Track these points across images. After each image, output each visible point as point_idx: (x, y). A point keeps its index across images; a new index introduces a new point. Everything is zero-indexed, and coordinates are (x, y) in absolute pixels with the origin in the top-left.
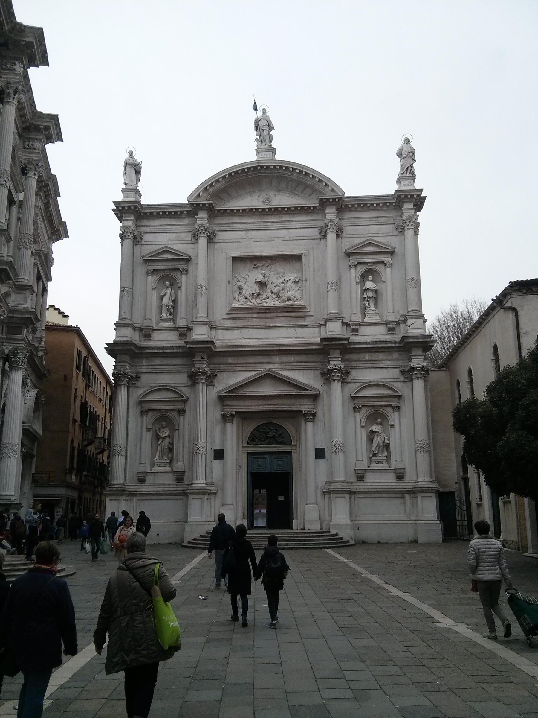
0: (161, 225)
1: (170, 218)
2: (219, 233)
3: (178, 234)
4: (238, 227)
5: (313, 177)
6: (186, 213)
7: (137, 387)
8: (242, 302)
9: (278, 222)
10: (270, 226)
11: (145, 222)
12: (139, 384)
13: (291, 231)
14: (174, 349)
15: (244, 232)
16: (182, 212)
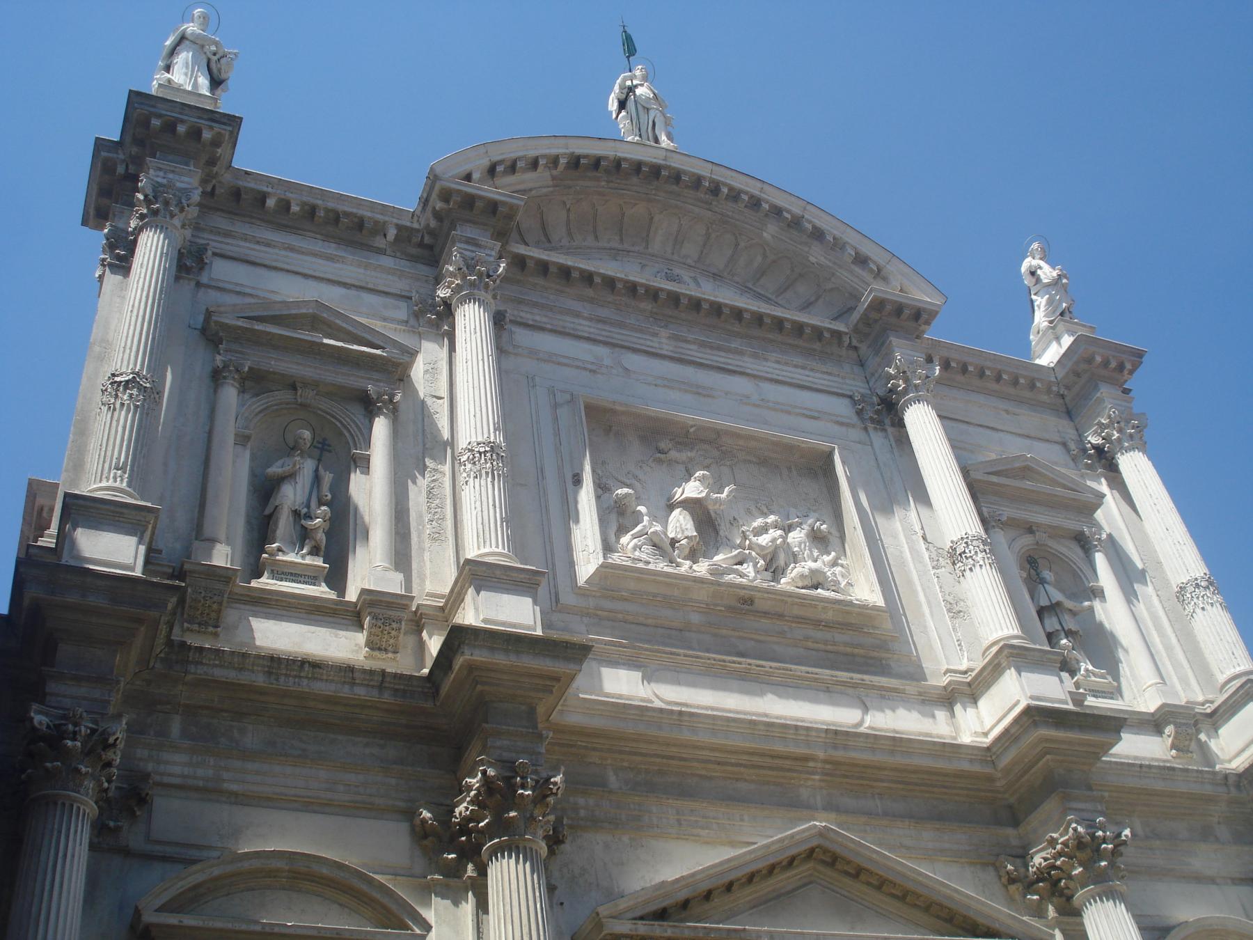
0: (291, 249)
1: (328, 238)
2: (516, 329)
3: (353, 292)
4: (585, 327)
5: (838, 245)
6: (392, 233)
7: (127, 852)
8: (644, 556)
9: (719, 348)
10: (693, 352)
11: (220, 222)
12: (134, 838)
13: (767, 386)
14: (353, 683)
15: (602, 351)
16: (379, 229)
